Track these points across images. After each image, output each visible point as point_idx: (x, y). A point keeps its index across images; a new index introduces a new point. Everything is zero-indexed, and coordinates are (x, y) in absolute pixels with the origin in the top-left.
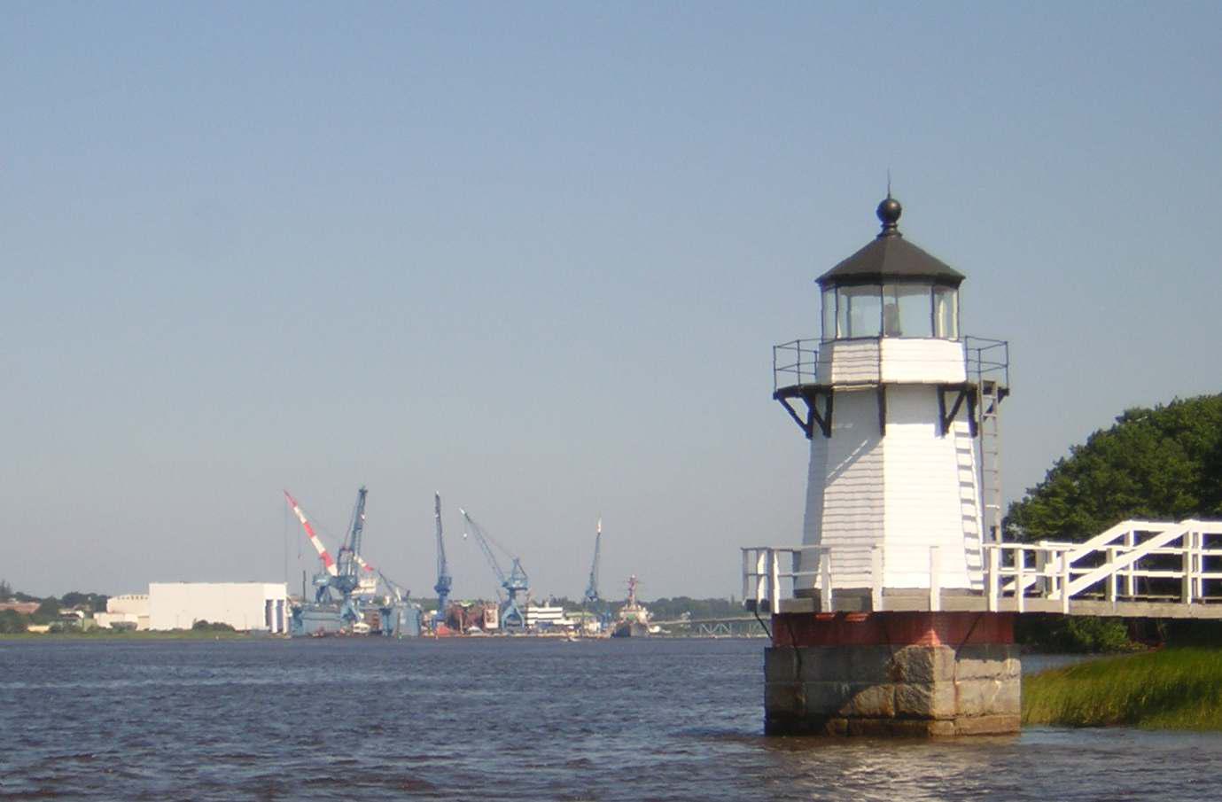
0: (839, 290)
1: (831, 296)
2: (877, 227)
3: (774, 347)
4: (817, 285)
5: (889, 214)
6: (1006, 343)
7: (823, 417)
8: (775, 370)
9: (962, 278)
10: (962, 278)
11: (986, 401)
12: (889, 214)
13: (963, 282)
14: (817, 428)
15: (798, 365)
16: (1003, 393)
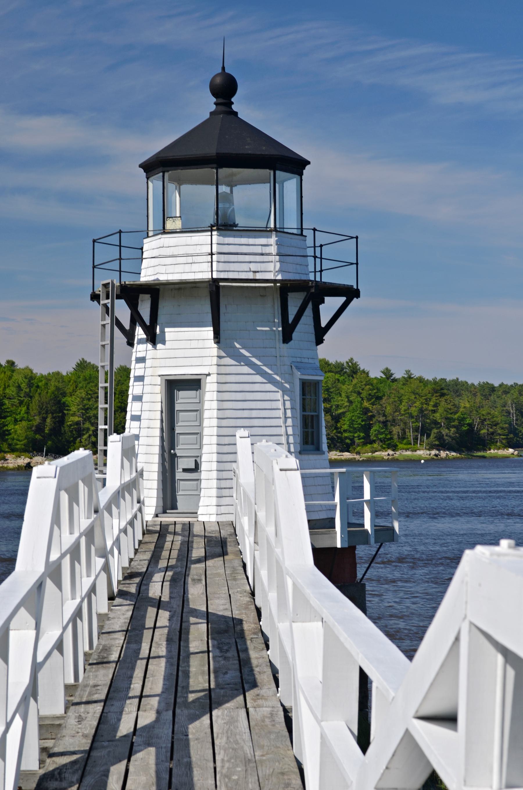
0: (166, 175)
1: (154, 185)
2: (209, 104)
3: (94, 241)
4: (142, 170)
5: (225, 89)
6: (357, 238)
7: (148, 323)
8: (94, 267)
9: (308, 163)
10: (308, 163)
11: (330, 305)
12: (225, 89)
13: (308, 167)
14: (140, 333)
15: (120, 259)
16: (351, 293)
